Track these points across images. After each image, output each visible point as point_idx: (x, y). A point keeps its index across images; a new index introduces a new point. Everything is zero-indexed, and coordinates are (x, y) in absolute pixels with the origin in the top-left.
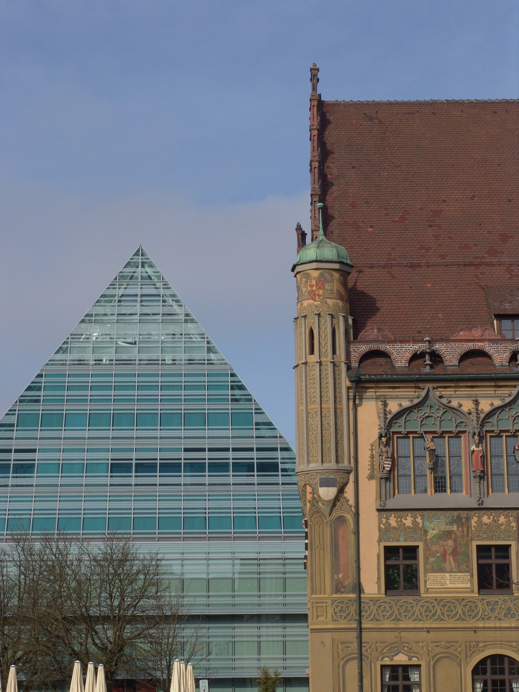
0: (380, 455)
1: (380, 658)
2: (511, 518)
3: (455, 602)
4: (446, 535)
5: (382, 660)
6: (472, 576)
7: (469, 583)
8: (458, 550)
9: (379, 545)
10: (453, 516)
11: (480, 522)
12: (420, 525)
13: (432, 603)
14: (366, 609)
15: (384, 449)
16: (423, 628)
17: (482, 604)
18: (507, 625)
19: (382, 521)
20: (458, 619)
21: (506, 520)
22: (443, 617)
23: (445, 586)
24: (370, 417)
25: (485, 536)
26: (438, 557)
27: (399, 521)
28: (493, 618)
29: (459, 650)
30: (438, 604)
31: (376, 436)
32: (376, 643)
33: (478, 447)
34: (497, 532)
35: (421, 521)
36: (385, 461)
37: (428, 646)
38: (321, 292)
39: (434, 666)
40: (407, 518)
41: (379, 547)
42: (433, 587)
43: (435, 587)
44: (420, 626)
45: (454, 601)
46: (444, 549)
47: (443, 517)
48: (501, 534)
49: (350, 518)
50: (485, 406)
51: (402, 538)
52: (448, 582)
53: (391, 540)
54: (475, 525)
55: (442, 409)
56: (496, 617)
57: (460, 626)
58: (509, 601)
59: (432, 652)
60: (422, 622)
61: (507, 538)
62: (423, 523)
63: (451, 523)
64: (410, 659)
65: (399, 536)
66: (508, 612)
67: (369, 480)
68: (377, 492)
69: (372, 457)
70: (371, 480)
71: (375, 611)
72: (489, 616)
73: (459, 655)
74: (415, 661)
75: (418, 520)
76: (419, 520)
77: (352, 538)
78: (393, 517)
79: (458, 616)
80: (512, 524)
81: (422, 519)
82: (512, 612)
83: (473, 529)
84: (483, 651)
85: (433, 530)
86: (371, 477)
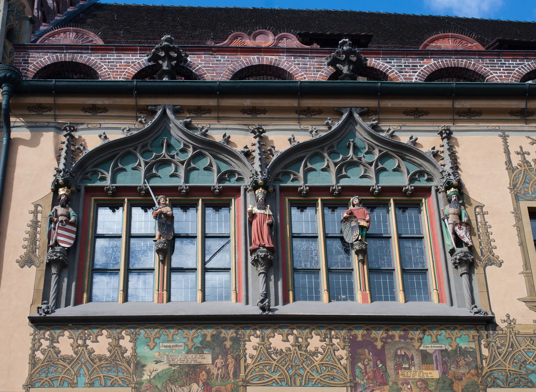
2: (335, 341)
4: (187, 374)
12: (128, 354)
15: (61, 210)
19: (41, 345)
21: (323, 343)
27: (79, 345)
31: (48, 189)
33: (265, 209)
35: (131, 345)
40: (99, 338)
47: (182, 337)
48: (314, 373)
53: (56, 383)
54: (255, 353)
55: (191, 149)
61: (327, 380)
62: (134, 349)
63: (199, 350)
65: (77, 375)
67: (22, 267)
68: (36, 290)
69: (35, 224)
70: (26, 267)
75: (122, 343)
76: (126, 343)
78: (65, 337)
80: (337, 353)
81: (134, 340)
83: (249, 361)
85: (157, 362)
86: (27, 261)
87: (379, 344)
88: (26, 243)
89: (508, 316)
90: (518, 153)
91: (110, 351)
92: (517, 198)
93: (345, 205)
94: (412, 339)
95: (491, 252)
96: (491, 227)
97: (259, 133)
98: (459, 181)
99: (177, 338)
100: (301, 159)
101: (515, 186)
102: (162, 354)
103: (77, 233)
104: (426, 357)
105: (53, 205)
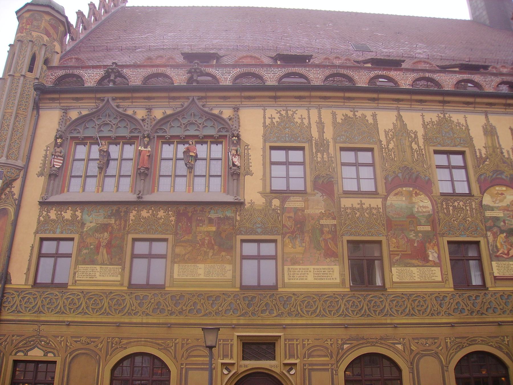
0: (52, 155)
1: (14, 353)
2: (170, 213)
3: (102, 295)
5: (15, 355)
6: (123, 269)
7: (119, 276)
8: (113, 242)
9: (35, 236)
10: (112, 210)
11: (138, 217)
13: (78, 295)
14: (9, 300)
16: (64, 322)
17: (131, 298)
18: (155, 321)
20: (103, 313)
22: (87, 311)
23: (94, 279)
24: (50, 121)
25: (142, 229)
26: (91, 249)
28: (140, 313)
29: (100, 346)
30: (84, 297)
31: (52, 139)
32: (13, 336)
33: (147, 148)
34: (155, 226)
36: (56, 159)
37: (67, 341)
38: (28, 27)
39: (70, 363)
41: (35, 239)
42: (81, 279)
43: (83, 279)
44: (61, 319)
45: (101, 294)
46: (99, 241)
49: (12, 210)
50: (158, 114)
51: (58, 230)
52: (98, 274)
53: (47, 232)
54: (134, 218)
56: (143, 312)
57: (104, 320)
58: (160, 296)
59: (70, 348)
60: (64, 315)
62: (82, 217)
63: (109, 217)
64: (45, 355)
66: (157, 307)
69: (46, 156)
71: (18, 302)
72: (137, 310)
73: (99, 352)
74: (50, 357)
75: (77, 213)
76: (78, 213)
77: (9, 229)
78: (53, 211)
79: (103, 310)
82: (161, 307)
83: (131, 222)
84: (126, 348)
85: (91, 222)
86: (40, 174)
87: (190, 214)
88: (41, 165)
89: (251, 200)
90: (269, 118)
91: (71, 217)
92: (265, 141)
93: (188, 143)
94: (205, 212)
95: (249, 169)
96: (250, 156)
97: (149, 110)
98: (238, 134)
99: (101, 211)
100: (168, 122)
101: (265, 135)
102: (92, 219)
103: (63, 160)
104: (211, 221)
105: (55, 147)
